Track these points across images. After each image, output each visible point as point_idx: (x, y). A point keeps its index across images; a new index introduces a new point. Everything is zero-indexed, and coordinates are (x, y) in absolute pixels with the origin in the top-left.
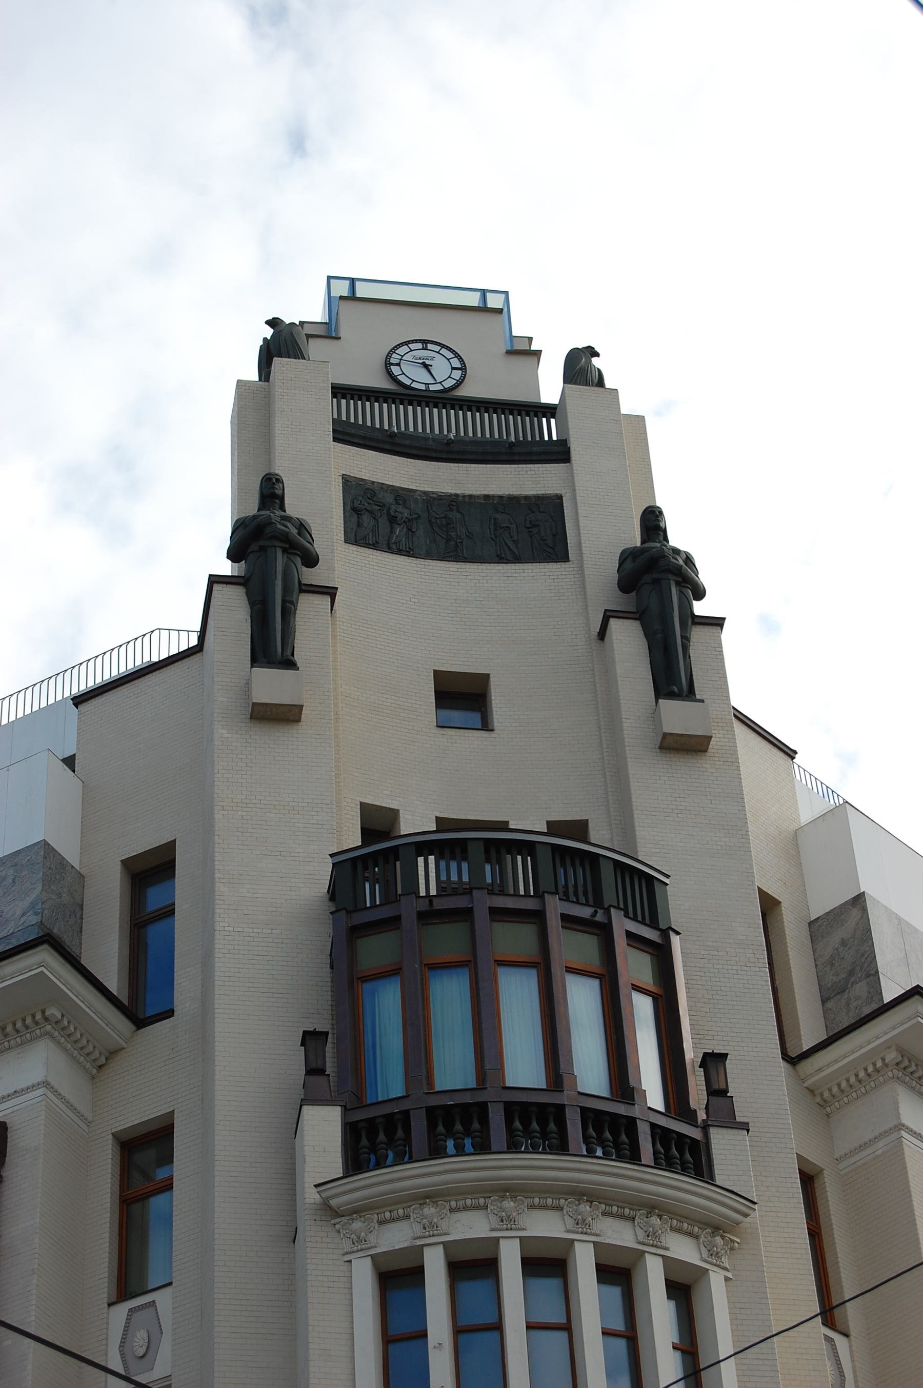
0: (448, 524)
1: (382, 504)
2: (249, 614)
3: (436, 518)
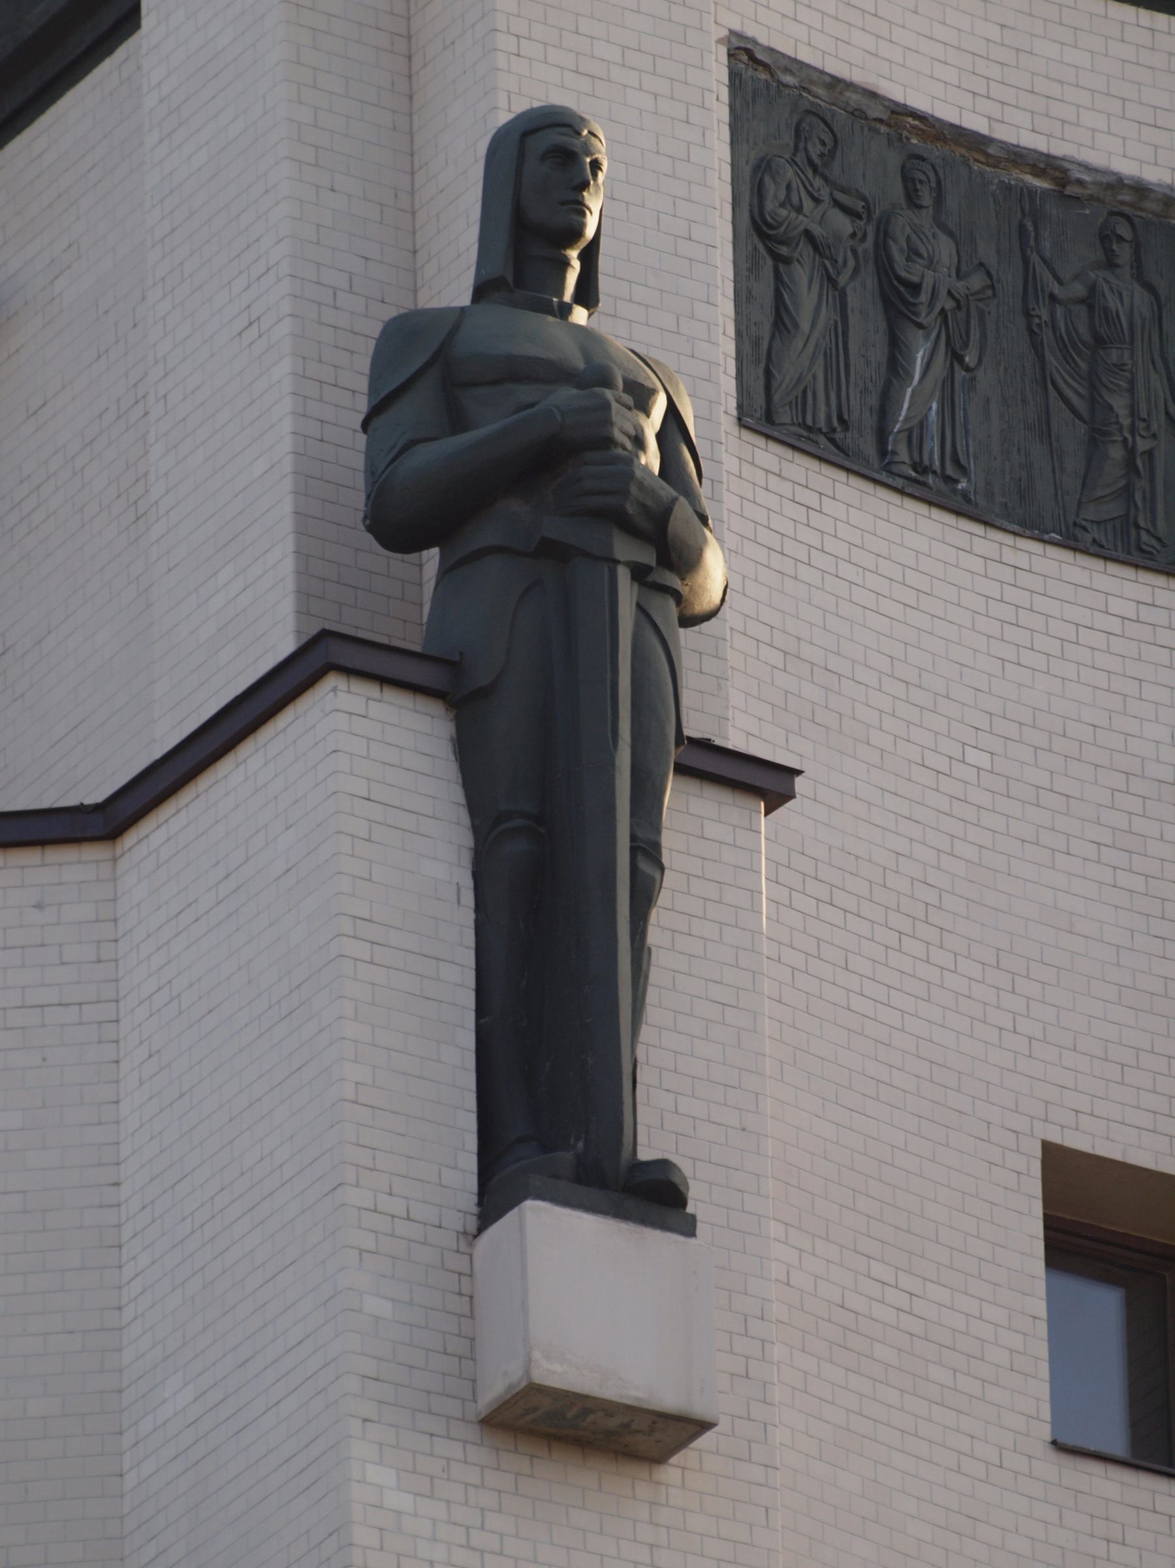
0: (1100, 342)
1: (859, 205)
2: (466, 859)
3: (1052, 297)
